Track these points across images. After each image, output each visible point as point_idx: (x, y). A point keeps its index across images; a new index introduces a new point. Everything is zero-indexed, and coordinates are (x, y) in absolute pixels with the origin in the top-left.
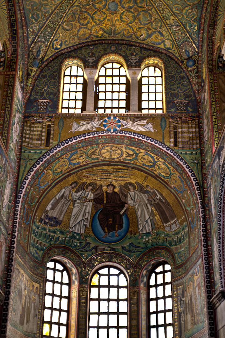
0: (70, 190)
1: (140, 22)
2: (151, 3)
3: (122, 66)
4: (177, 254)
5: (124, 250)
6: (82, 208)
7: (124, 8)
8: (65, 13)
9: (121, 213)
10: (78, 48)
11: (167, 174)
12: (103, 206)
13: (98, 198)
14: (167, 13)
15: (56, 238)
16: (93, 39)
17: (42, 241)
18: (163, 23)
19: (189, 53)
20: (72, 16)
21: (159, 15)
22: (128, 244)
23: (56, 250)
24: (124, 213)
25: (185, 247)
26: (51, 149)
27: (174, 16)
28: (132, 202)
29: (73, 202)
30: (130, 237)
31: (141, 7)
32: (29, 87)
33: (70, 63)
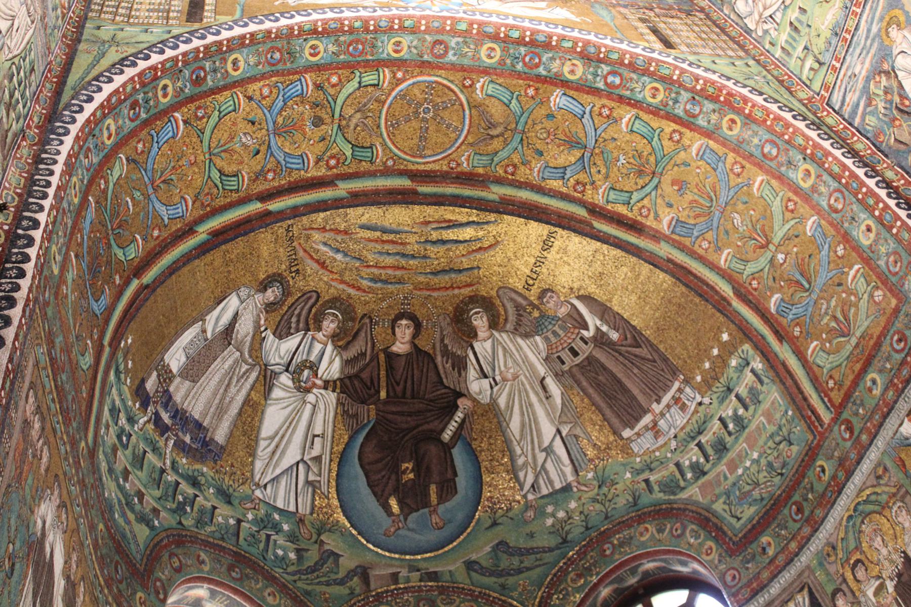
0: (259, 315)
4: (722, 500)
5: (476, 571)
6: (298, 411)
9: (447, 435)
11: (640, 173)
12: (377, 410)
13: (357, 376)
15: (202, 511)
17: (145, 486)
22: (488, 549)
23: (203, 556)
24: (455, 434)
25: (761, 442)
26: (210, 27)
28: (485, 383)
29: (265, 377)
30: (489, 522)
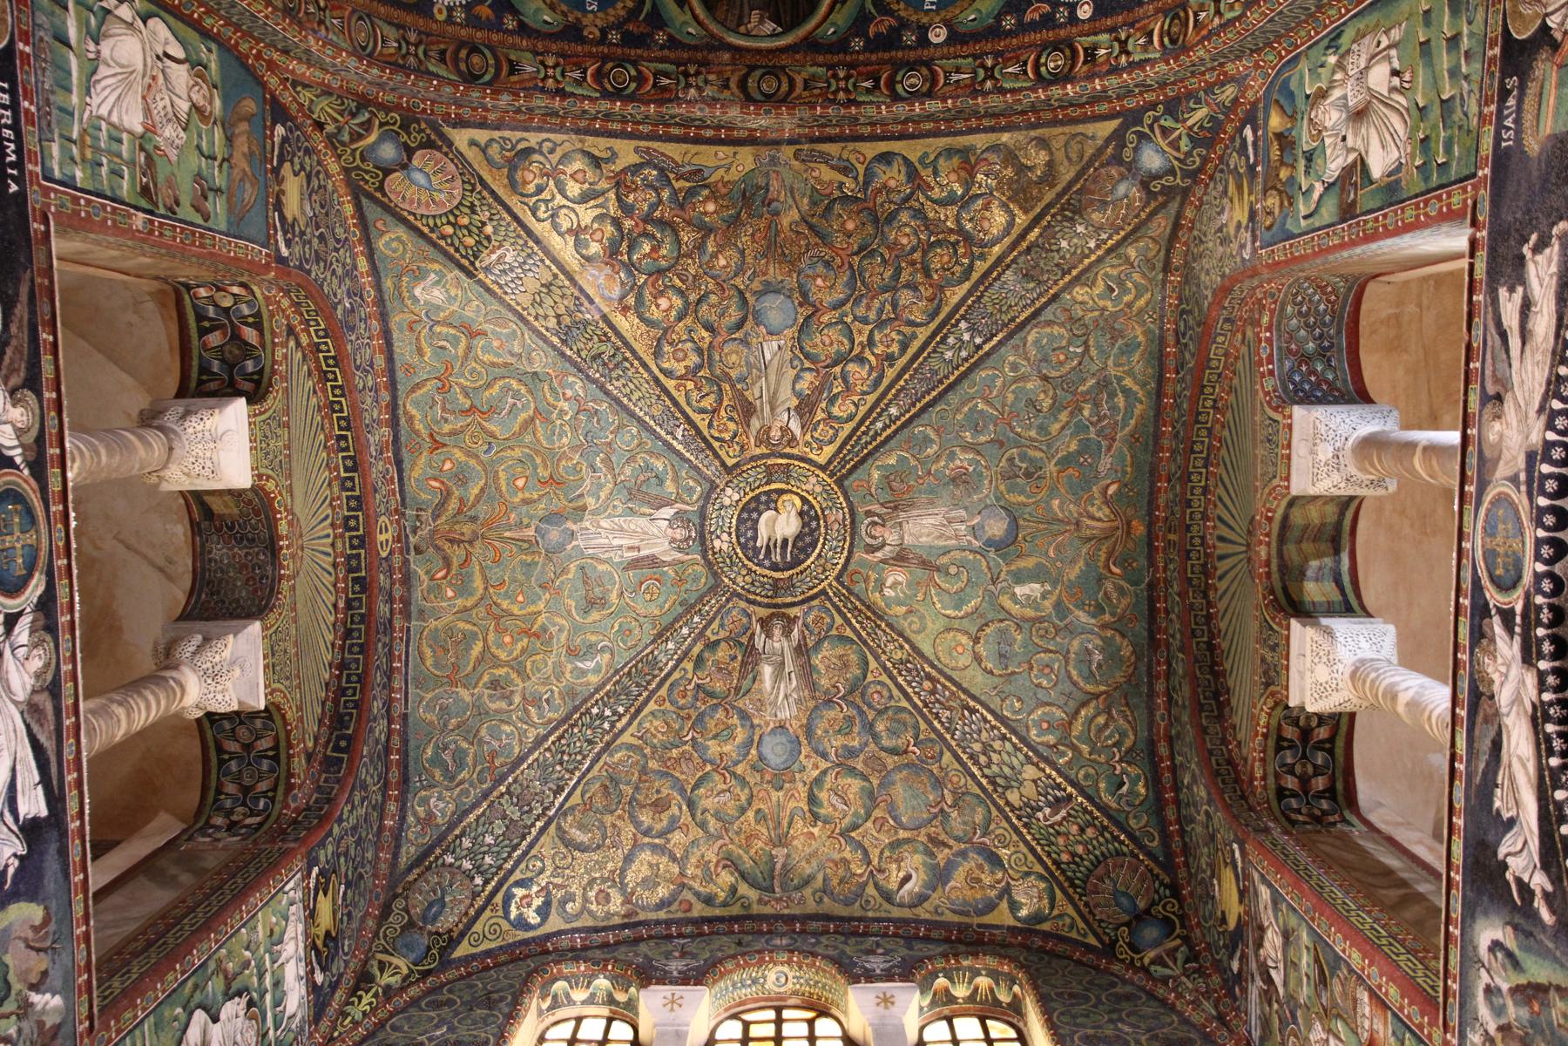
1: (894, 819)
2: (934, 730)
3: (824, 1013)
7: (824, 756)
8: (577, 774)
10: (618, 943)
14: (1006, 757)
16: (689, 910)
18: (993, 809)
19: (1132, 900)
20: (606, 787)
21: (973, 776)
27: (1037, 765)
31: (893, 751)
32: (356, 1024)
33: (579, 995)
